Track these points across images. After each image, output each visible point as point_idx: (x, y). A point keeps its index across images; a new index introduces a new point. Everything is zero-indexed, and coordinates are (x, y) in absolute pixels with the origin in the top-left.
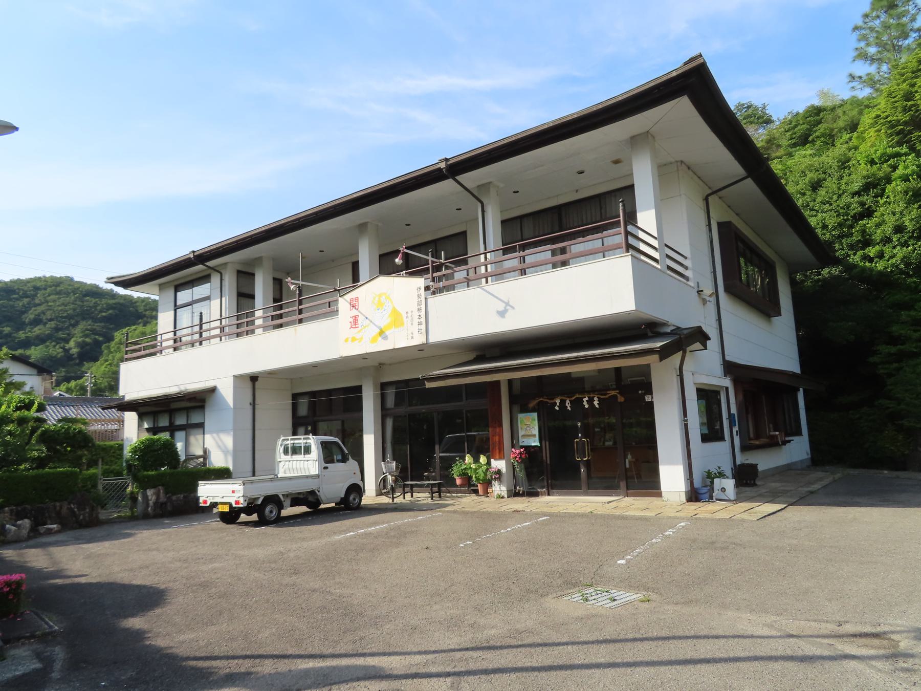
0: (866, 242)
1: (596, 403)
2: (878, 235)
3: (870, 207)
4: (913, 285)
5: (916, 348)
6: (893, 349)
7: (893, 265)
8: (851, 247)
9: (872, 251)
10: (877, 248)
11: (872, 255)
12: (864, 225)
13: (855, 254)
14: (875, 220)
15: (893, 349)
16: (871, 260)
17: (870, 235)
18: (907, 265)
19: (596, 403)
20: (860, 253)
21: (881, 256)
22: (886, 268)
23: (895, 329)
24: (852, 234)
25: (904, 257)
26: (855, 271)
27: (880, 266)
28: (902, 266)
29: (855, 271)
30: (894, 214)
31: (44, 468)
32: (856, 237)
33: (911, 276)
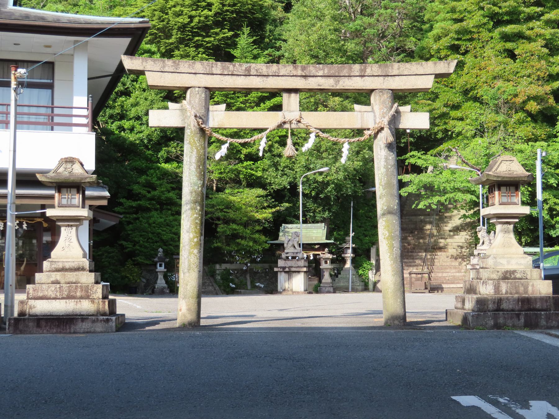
0: (122, 117)
1: (25, 226)
2: (132, 113)
3: (128, 88)
4: (150, 156)
5: (149, 204)
6: (134, 204)
7: (139, 139)
8: (111, 117)
9: (127, 124)
10: (131, 122)
11: (126, 127)
12: (123, 102)
13: (112, 123)
14: (131, 100)
15: (134, 204)
16: (124, 130)
17: (127, 111)
18: (150, 140)
19: (25, 226)
20: (117, 123)
21: (132, 129)
22: (135, 140)
23: (136, 188)
24: (115, 107)
25: (149, 135)
26: (112, 137)
27: (132, 137)
28: (146, 141)
29: (112, 137)
30: (146, 99)
31: (202, 31)
32: (117, 111)
33: (149, 149)
